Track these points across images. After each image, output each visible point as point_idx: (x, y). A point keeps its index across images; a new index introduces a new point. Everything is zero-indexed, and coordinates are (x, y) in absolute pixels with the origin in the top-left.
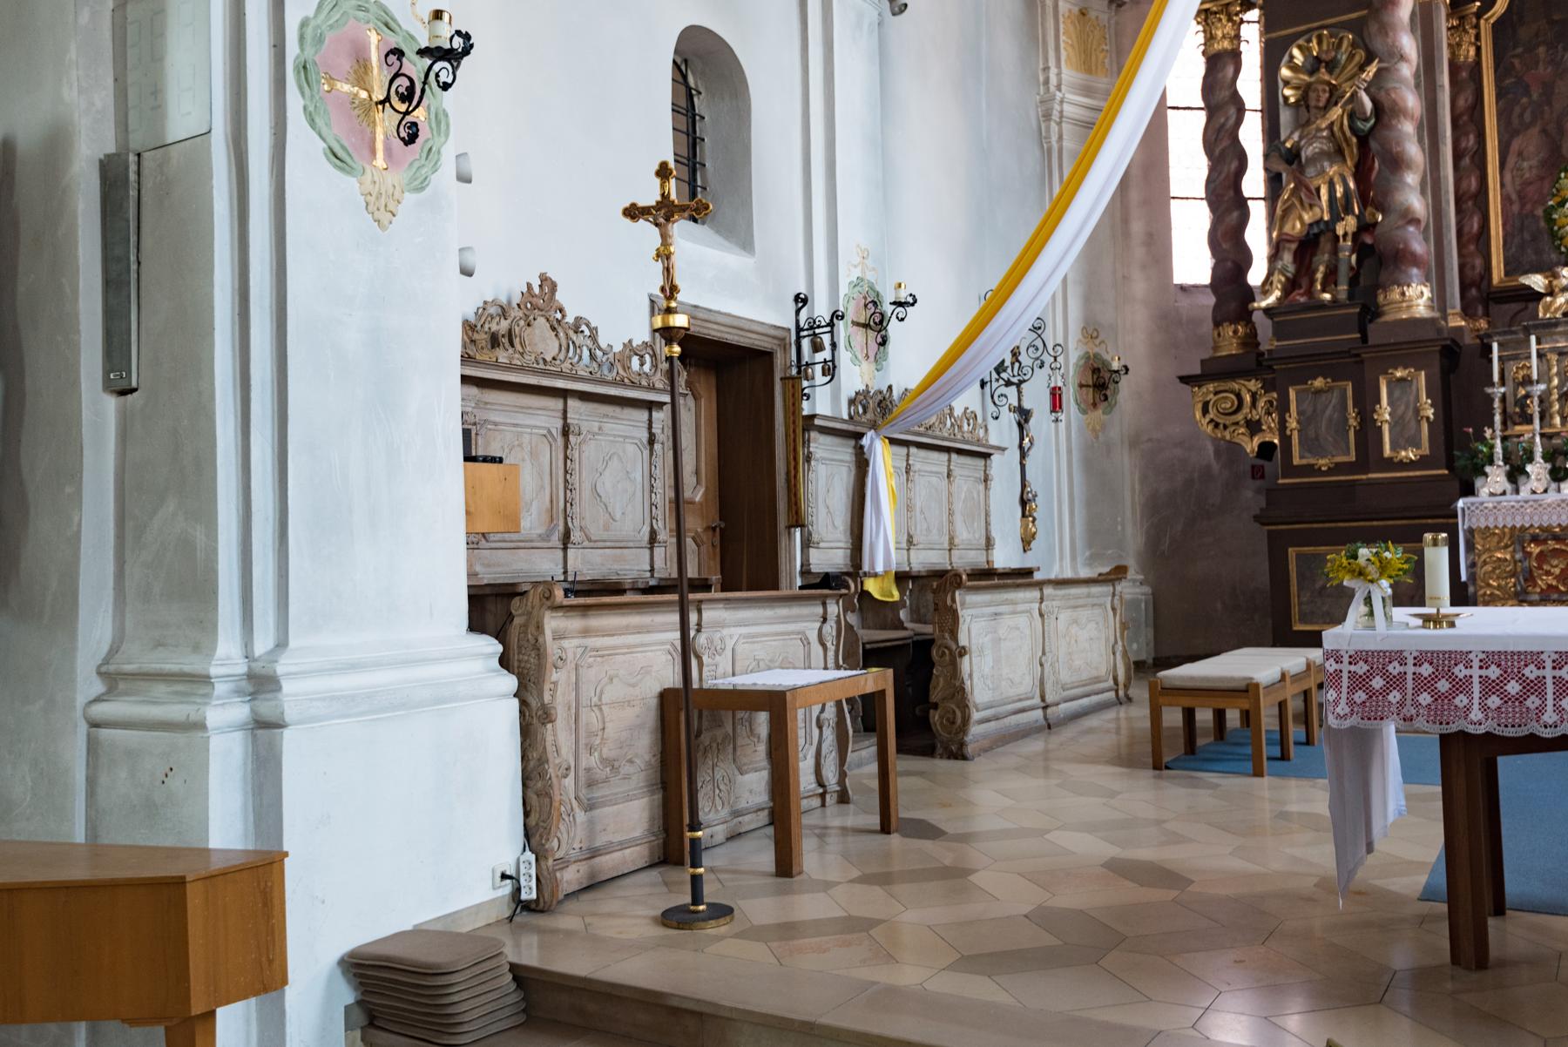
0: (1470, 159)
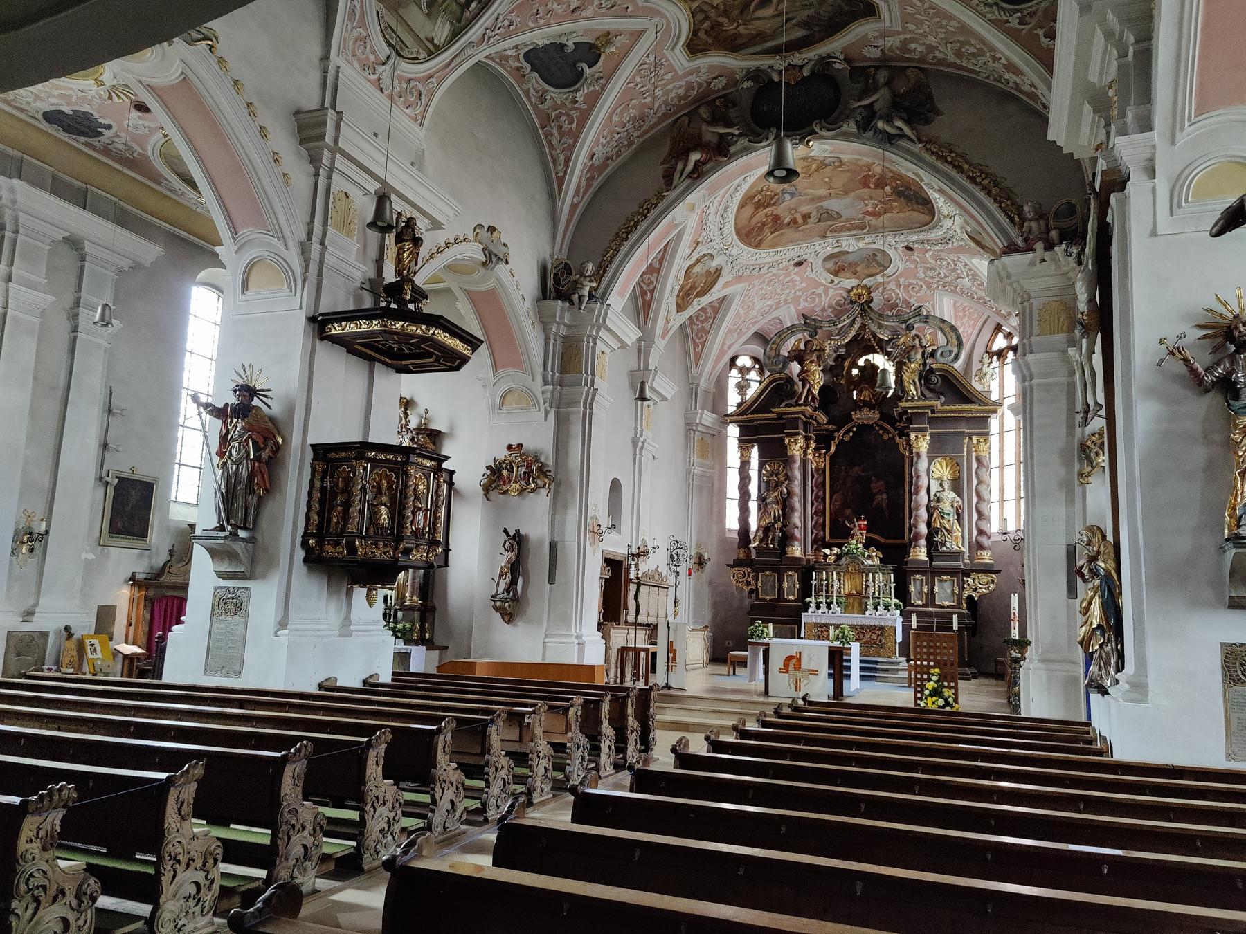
0: (819, 499)
